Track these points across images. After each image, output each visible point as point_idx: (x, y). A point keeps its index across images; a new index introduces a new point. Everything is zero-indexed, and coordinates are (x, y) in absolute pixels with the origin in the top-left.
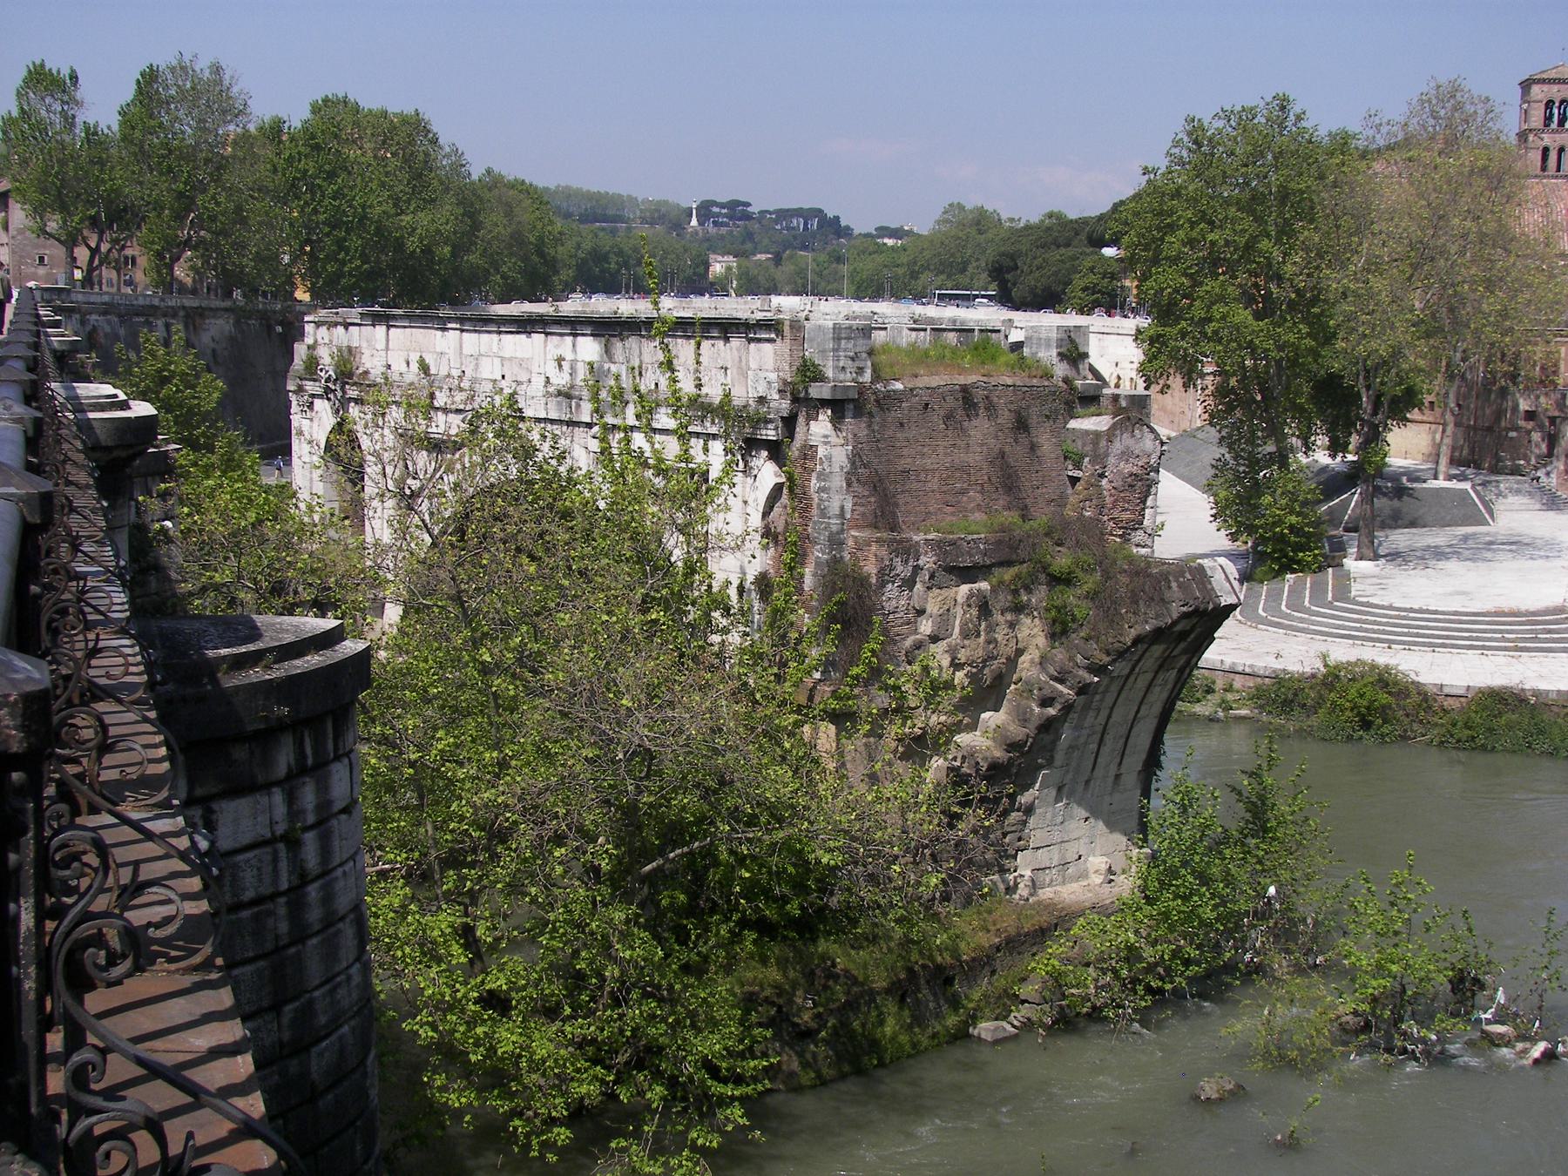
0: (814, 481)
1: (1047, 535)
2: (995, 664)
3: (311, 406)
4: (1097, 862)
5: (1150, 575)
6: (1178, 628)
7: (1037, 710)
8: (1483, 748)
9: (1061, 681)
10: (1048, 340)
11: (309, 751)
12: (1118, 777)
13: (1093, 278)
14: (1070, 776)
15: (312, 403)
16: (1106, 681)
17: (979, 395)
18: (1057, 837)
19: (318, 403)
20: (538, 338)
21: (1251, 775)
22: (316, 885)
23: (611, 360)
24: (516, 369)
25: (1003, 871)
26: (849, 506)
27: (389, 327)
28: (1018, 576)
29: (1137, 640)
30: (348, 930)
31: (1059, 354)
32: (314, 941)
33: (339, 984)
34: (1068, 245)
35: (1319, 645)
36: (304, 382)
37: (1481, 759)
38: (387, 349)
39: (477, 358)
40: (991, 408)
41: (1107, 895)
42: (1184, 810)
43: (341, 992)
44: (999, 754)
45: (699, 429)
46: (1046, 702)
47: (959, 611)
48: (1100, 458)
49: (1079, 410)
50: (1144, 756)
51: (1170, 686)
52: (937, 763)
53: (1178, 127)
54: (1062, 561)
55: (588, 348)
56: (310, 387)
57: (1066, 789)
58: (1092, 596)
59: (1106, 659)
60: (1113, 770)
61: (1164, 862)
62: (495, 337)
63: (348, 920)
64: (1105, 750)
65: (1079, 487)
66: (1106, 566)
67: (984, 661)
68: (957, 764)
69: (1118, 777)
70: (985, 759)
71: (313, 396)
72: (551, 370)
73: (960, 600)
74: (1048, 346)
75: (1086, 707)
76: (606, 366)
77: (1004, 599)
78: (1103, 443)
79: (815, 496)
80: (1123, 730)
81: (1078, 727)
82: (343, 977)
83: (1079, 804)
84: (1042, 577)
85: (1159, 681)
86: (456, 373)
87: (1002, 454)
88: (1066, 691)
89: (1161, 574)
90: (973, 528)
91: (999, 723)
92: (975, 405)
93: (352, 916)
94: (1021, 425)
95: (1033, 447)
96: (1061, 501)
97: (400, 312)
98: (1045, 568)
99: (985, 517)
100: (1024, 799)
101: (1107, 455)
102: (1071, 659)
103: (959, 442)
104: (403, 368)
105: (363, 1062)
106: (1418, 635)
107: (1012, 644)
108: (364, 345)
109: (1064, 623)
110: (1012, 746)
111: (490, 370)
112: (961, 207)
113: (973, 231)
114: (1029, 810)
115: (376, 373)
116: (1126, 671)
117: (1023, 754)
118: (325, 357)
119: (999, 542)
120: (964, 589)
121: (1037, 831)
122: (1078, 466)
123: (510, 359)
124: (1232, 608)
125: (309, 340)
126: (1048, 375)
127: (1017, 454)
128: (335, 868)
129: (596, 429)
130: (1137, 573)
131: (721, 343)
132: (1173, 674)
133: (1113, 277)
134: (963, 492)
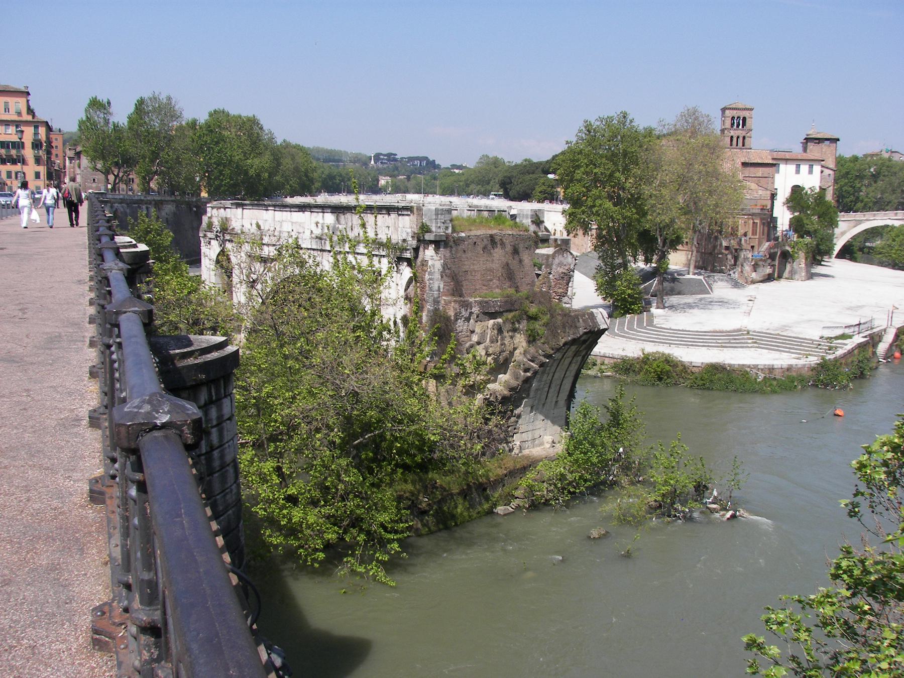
0: (427, 275)
1: (527, 298)
2: (504, 354)
3: (209, 243)
4: (548, 438)
5: (570, 316)
6: (582, 339)
7: (522, 374)
8: (708, 389)
9: (533, 361)
10: (527, 215)
11: (213, 394)
12: (556, 402)
13: (544, 188)
14: (537, 401)
16: (552, 361)
17: (497, 238)
18: (531, 428)
19: (212, 241)
20: (307, 214)
21: (613, 400)
22: (217, 451)
23: (339, 223)
24: (298, 227)
25: (507, 443)
26: (442, 286)
27: (243, 209)
28: (514, 316)
29: (565, 344)
30: (230, 470)
31: (532, 221)
32: (217, 475)
33: (227, 493)
34: (533, 173)
35: (641, 345)
37: (706, 393)
38: (242, 218)
39: (281, 222)
40: (503, 244)
41: (552, 452)
42: (585, 416)
43: (228, 497)
44: (506, 392)
45: (377, 253)
46: (526, 370)
47: (489, 331)
48: (549, 266)
49: (540, 245)
50: (567, 393)
51: (579, 363)
52: (480, 396)
53: (580, 124)
54: (533, 310)
55: (329, 218)
56: (209, 235)
57: (534, 408)
58: (546, 325)
59: (552, 352)
60: (554, 400)
61: (576, 438)
62: (289, 213)
63: (230, 466)
64: (551, 391)
65: (540, 278)
66: (552, 312)
67: (500, 353)
68: (488, 397)
69: (556, 402)
70: (500, 395)
71: (210, 239)
72: (313, 227)
73: (490, 327)
74: (527, 218)
75: (543, 372)
76: (337, 226)
77: (508, 326)
78: (551, 259)
79: (427, 282)
80: (559, 382)
81: (540, 381)
82: (229, 490)
83: (540, 413)
84: (525, 317)
85: (574, 361)
86: (272, 229)
87: (507, 264)
88: (535, 365)
89: (575, 315)
90: (495, 296)
91: (506, 379)
92: (496, 243)
93: (232, 464)
94: (516, 251)
95: (521, 261)
96: (532, 284)
97: (248, 202)
98: (526, 313)
99: (500, 291)
100: (517, 412)
101: (552, 264)
102: (537, 352)
103: (489, 259)
104: (249, 226)
105: (237, 526)
106: (681, 341)
107: (512, 346)
108: (233, 217)
109: (534, 337)
110: (512, 389)
111: (287, 227)
112: (488, 157)
113: (493, 167)
114: (519, 416)
115: (238, 229)
116: (560, 357)
117: (516, 393)
118: (216, 222)
119: (506, 302)
120: (492, 322)
121: (523, 425)
122: (540, 269)
123: (296, 223)
124: (605, 330)
125: (209, 215)
126: (527, 230)
127: (514, 264)
128: (224, 444)
129: (332, 253)
130: (565, 315)
131: (386, 216)
132: (580, 358)
133: (553, 187)
134: (491, 280)
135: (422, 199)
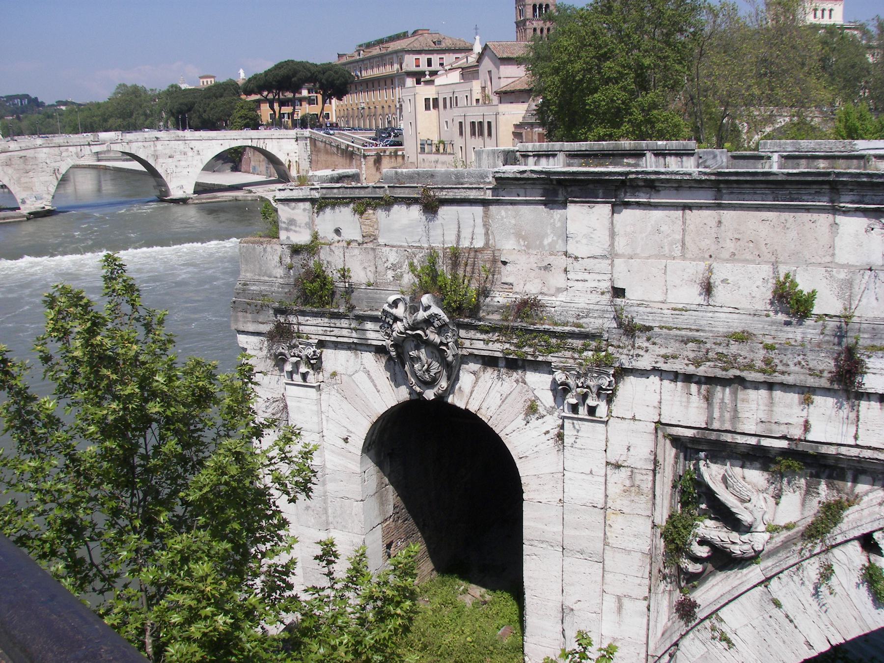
3: (316, 364)
13: (242, 112)
15: (319, 359)
34: (221, 96)
36: (292, 319)
71: (322, 344)
108: (508, 246)
112: (124, 85)
113: (133, 96)
135: (120, 137)
